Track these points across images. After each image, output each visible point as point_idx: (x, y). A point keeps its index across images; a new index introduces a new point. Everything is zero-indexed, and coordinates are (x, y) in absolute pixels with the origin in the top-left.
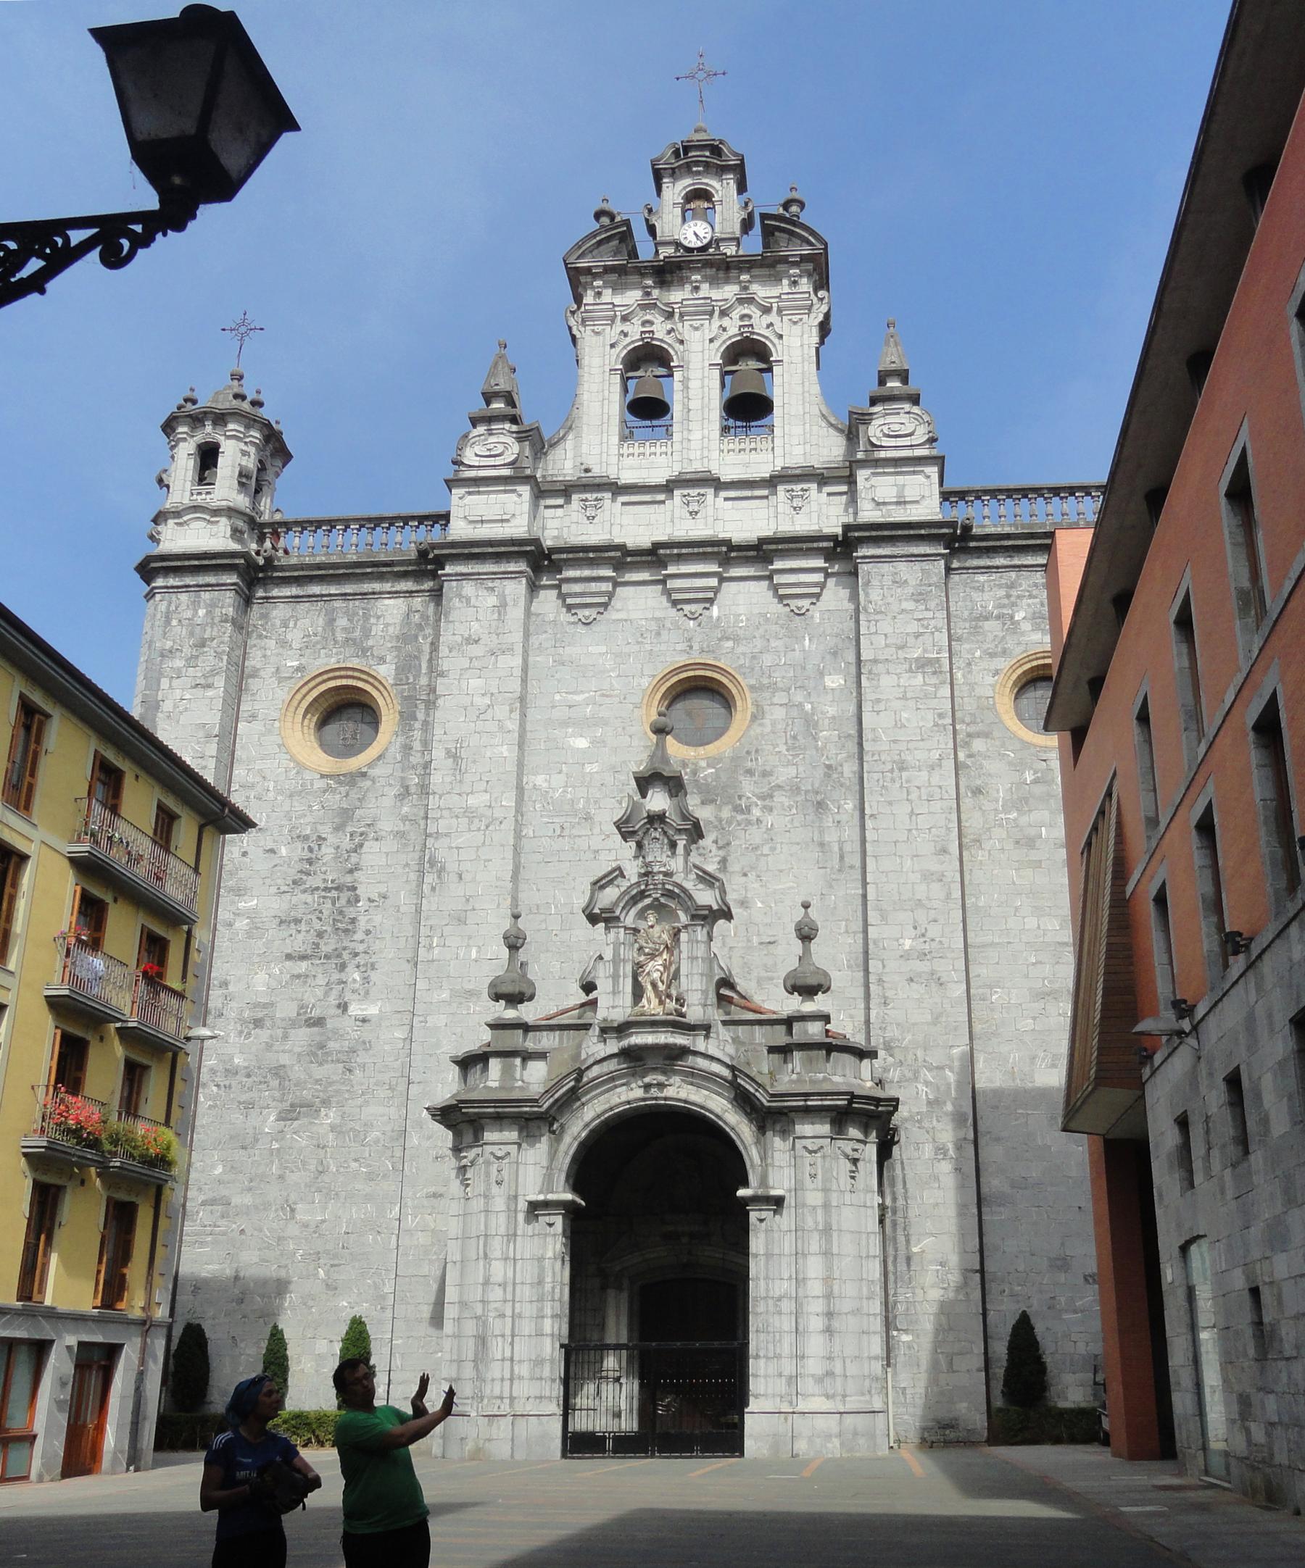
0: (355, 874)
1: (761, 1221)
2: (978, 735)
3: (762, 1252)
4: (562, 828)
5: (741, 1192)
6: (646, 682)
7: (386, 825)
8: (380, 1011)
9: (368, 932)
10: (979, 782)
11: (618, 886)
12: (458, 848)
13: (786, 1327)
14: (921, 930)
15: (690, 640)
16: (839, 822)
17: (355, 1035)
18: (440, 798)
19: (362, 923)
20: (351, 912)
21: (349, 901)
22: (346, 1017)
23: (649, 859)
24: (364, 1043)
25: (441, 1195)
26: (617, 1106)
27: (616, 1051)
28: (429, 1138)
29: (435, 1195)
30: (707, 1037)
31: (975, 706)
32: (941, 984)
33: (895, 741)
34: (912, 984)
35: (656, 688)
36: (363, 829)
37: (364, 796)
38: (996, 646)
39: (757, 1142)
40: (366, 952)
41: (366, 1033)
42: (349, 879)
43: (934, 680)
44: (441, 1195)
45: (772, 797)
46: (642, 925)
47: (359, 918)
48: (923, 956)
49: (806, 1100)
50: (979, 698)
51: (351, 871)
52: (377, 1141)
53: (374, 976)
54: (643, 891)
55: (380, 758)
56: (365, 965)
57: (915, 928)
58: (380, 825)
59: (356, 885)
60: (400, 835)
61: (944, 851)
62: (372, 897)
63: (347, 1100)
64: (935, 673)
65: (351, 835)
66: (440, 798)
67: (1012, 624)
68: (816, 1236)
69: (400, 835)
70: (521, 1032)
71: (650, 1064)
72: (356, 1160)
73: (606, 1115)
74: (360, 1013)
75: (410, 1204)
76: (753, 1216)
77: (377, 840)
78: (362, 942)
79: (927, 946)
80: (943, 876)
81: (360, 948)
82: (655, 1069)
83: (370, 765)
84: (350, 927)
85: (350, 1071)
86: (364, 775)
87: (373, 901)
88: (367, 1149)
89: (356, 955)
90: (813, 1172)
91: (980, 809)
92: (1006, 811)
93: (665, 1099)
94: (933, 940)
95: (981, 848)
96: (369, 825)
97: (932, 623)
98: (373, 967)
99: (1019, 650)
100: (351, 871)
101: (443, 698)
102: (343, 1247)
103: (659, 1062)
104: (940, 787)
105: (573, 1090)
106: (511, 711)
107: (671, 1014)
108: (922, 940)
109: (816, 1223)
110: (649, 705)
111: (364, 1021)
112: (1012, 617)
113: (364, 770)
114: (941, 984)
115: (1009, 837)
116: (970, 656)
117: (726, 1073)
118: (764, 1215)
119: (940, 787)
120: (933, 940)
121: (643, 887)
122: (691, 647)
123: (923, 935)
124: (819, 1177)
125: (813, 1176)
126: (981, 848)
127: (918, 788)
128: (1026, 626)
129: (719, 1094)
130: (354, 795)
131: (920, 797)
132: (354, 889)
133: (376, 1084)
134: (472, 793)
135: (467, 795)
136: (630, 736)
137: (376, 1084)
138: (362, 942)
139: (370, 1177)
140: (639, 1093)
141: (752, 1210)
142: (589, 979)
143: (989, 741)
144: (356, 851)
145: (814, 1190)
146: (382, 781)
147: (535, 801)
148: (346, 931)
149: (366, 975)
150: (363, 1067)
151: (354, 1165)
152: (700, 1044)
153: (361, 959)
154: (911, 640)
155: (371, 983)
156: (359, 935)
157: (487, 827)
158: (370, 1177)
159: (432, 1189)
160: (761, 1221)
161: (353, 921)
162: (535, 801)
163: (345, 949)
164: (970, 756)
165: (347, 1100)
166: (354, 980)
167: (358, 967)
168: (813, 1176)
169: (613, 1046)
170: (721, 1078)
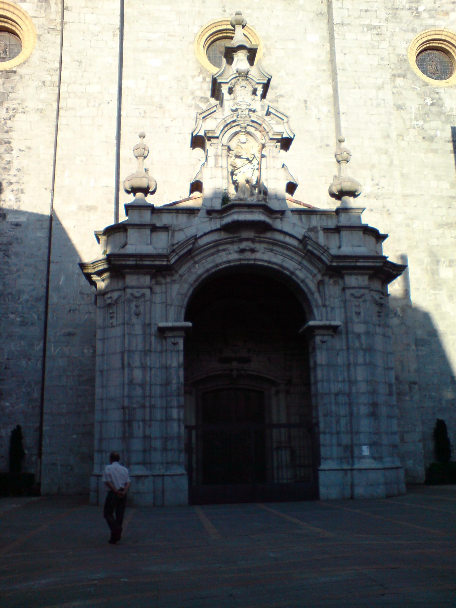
0: (10, 133)
1: (323, 342)
2: (399, 76)
3: (324, 363)
4: (145, 112)
5: (311, 323)
6: (197, 29)
7: (30, 104)
8: (28, 219)
9: (19, 170)
10: (400, 103)
11: (216, 119)
12: (81, 117)
13: (342, 412)
14: (376, 182)
15: (224, 7)
16: (319, 119)
17: (12, 234)
18: (68, 86)
19: (16, 164)
20: (7, 157)
21: (6, 150)
22: (4, 222)
23: (239, 99)
24: (17, 239)
25: (74, 335)
26: (220, 264)
27: (218, 226)
28: (64, 298)
29: (69, 334)
30: (281, 220)
31: (397, 59)
32: (389, 214)
33: (356, 72)
34: (372, 213)
35: (203, 34)
36: (14, 106)
37: (16, 85)
38: (408, 26)
39: (319, 290)
40: (18, 183)
41: (18, 233)
42: (6, 136)
43: (377, 38)
44: (74, 335)
45: (277, 101)
46: (233, 144)
47: (13, 161)
48: (377, 197)
49: (356, 262)
50: (399, 55)
51: (7, 132)
52: (27, 301)
53: (23, 197)
54: (234, 121)
55: (24, 63)
56: (18, 190)
57: (373, 180)
58: (26, 104)
59: (10, 140)
60: (40, 111)
61: (388, 136)
62: (21, 149)
63: (6, 275)
64: (378, 34)
65: (7, 109)
66: (68, 86)
67: (417, 13)
68: (361, 353)
69: (40, 111)
70: (149, 212)
71: (245, 234)
72: (13, 313)
73: (213, 270)
74: (14, 220)
75: (52, 339)
76: (318, 339)
77: (24, 113)
78: (15, 176)
79: (380, 191)
80: (388, 151)
81: (14, 180)
82: (247, 240)
83: (20, 66)
84: (7, 166)
85: (8, 256)
86: (15, 72)
87: (22, 151)
88: (21, 306)
89: (11, 183)
90: (357, 310)
91: (402, 118)
92: (416, 119)
93: (255, 260)
94: (383, 188)
95: (403, 140)
96: (19, 104)
97: (376, 5)
98: (22, 192)
99: (419, 29)
100: (7, 132)
101: (68, 24)
102: (6, 368)
103: (251, 234)
104: (384, 100)
105: (190, 252)
106: (114, 36)
107: (261, 201)
108: (377, 187)
109: (361, 345)
110: (198, 43)
111: (17, 225)
112: (417, 9)
113: (14, 69)
114: (389, 214)
115: (419, 134)
116: (393, 31)
117: (295, 243)
118: (325, 338)
119: (384, 100)
120: (383, 188)
121: (235, 118)
122: (225, 11)
123: (378, 185)
124: (362, 314)
125: (358, 314)
126: (403, 140)
127: (371, 99)
128: (425, 15)
129: (291, 259)
130: (8, 85)
131: (372, 105)
132: (9, 143)
133: (26, 265)
134: (89, 84)
135: (86, 85)
136: (187, 61)
137: (26, 265)
138: (15, 176)
139: (23, 323)
140: (235, 256)
141: (318, 335)
142: (197, 179)
143: (405, 80)
144: (10, 119)
145: (359, 322)
146: (27, 77)
147: (127, 95)
148: (5, 169)
149: (18, 197)
150: (16, 254)
151: (12, 316)
152: (278, 224)
153: (15, 187)
154: (363, 14)
155: (22, 202)
156: (13, 172)
157: (99, 105)
158: (23, 323)
159: (67, 331)
160: (323, 342)
161: (9, 162)
162: (127, 95)
163: (4, 180)
164: (395, 87)
165: (6, 275)
166: (10, 200)
167: (13, 191)
168: (358, 314)
169: (217, 224)
170: (295, 247)
